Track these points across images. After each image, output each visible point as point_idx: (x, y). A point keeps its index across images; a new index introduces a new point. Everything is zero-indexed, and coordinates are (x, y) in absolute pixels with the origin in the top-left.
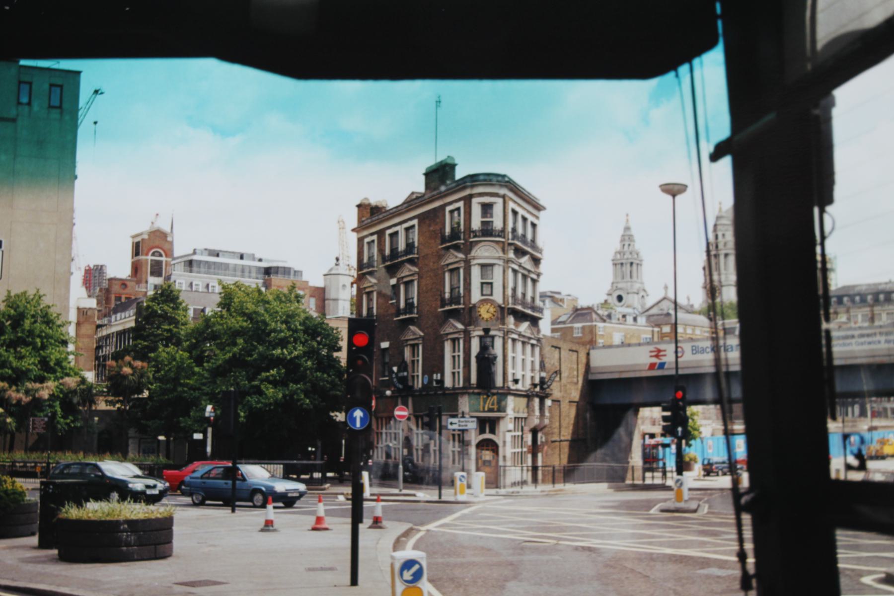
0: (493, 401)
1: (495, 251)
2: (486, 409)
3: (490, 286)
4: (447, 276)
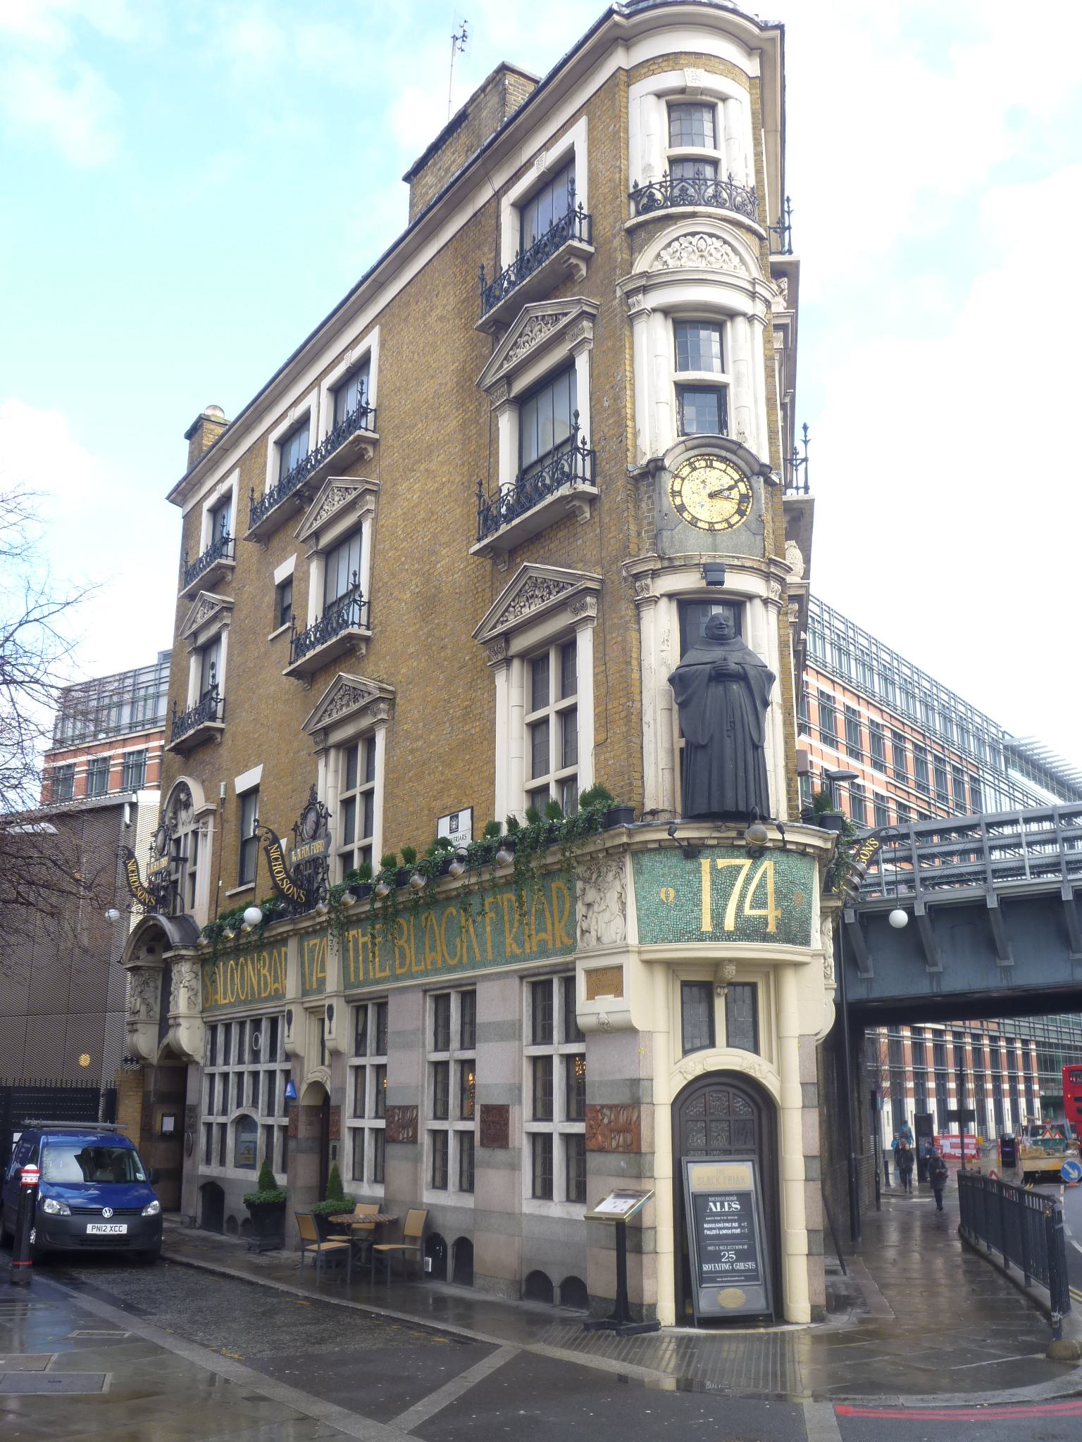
0: (762, 885)
1: (736, 260)
2: (729, 924)
3: (712, 399)
4: (506, 425)
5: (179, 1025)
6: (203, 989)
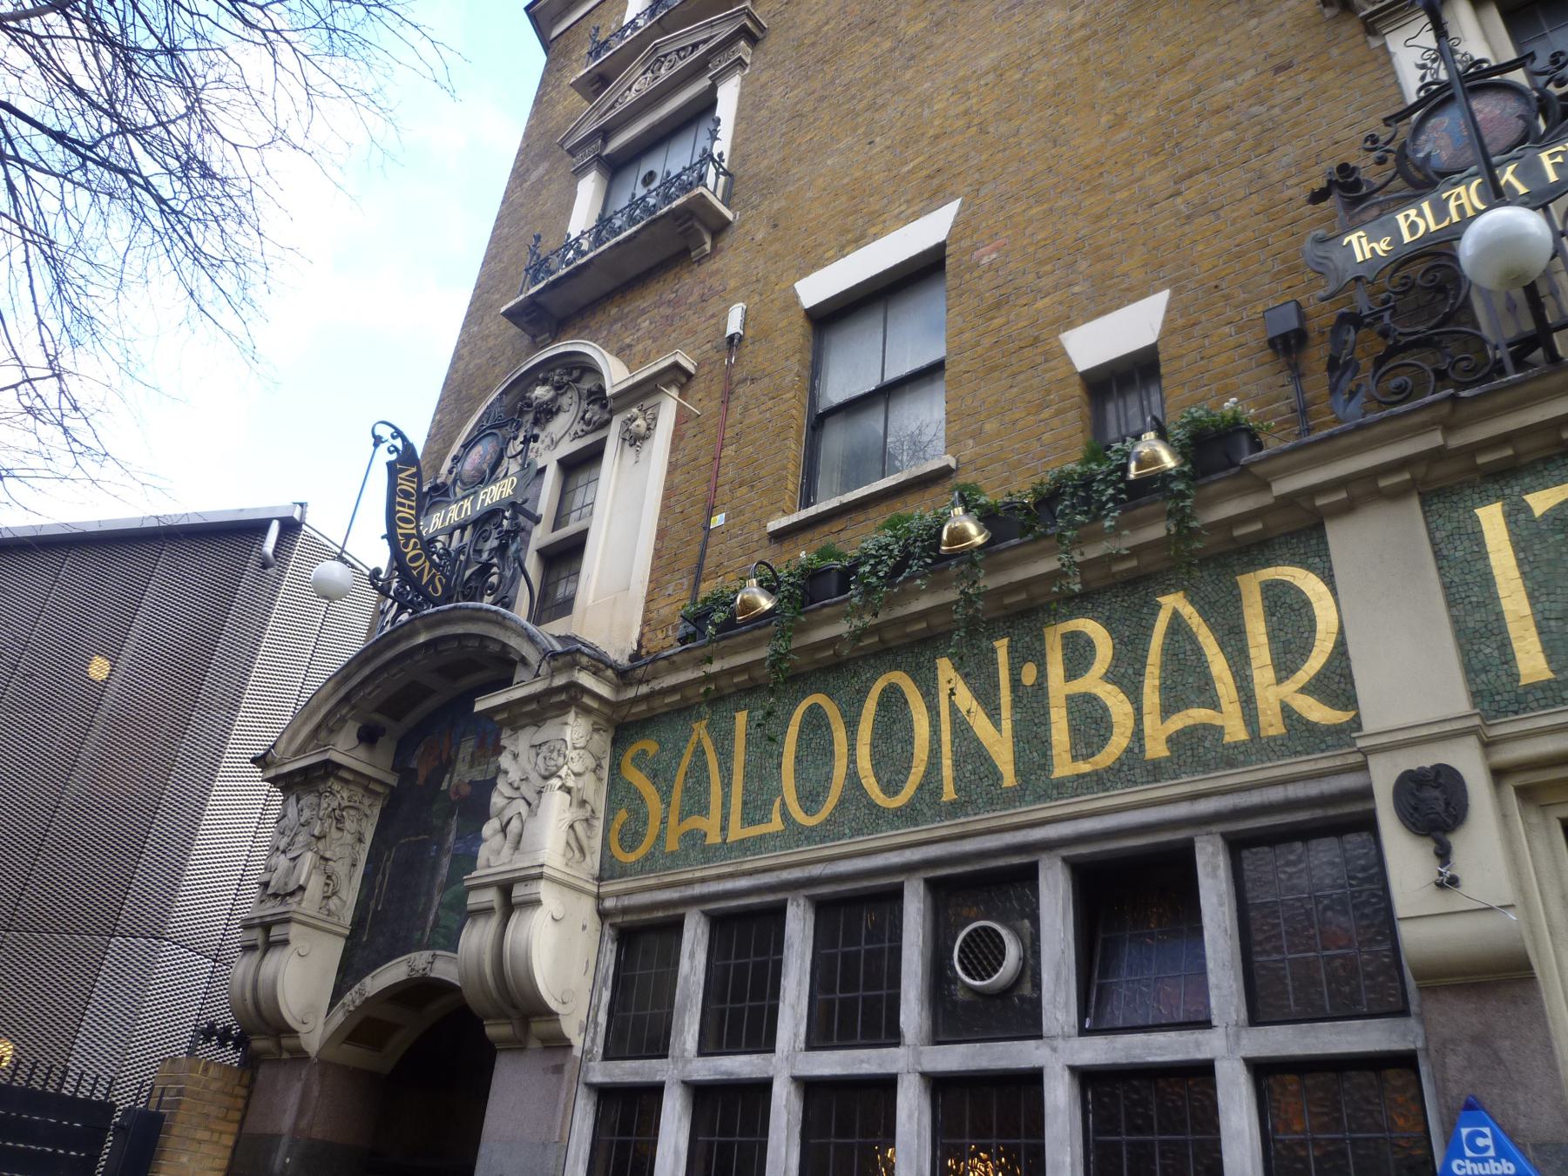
5: (536, 903)
6: (611, 810)
